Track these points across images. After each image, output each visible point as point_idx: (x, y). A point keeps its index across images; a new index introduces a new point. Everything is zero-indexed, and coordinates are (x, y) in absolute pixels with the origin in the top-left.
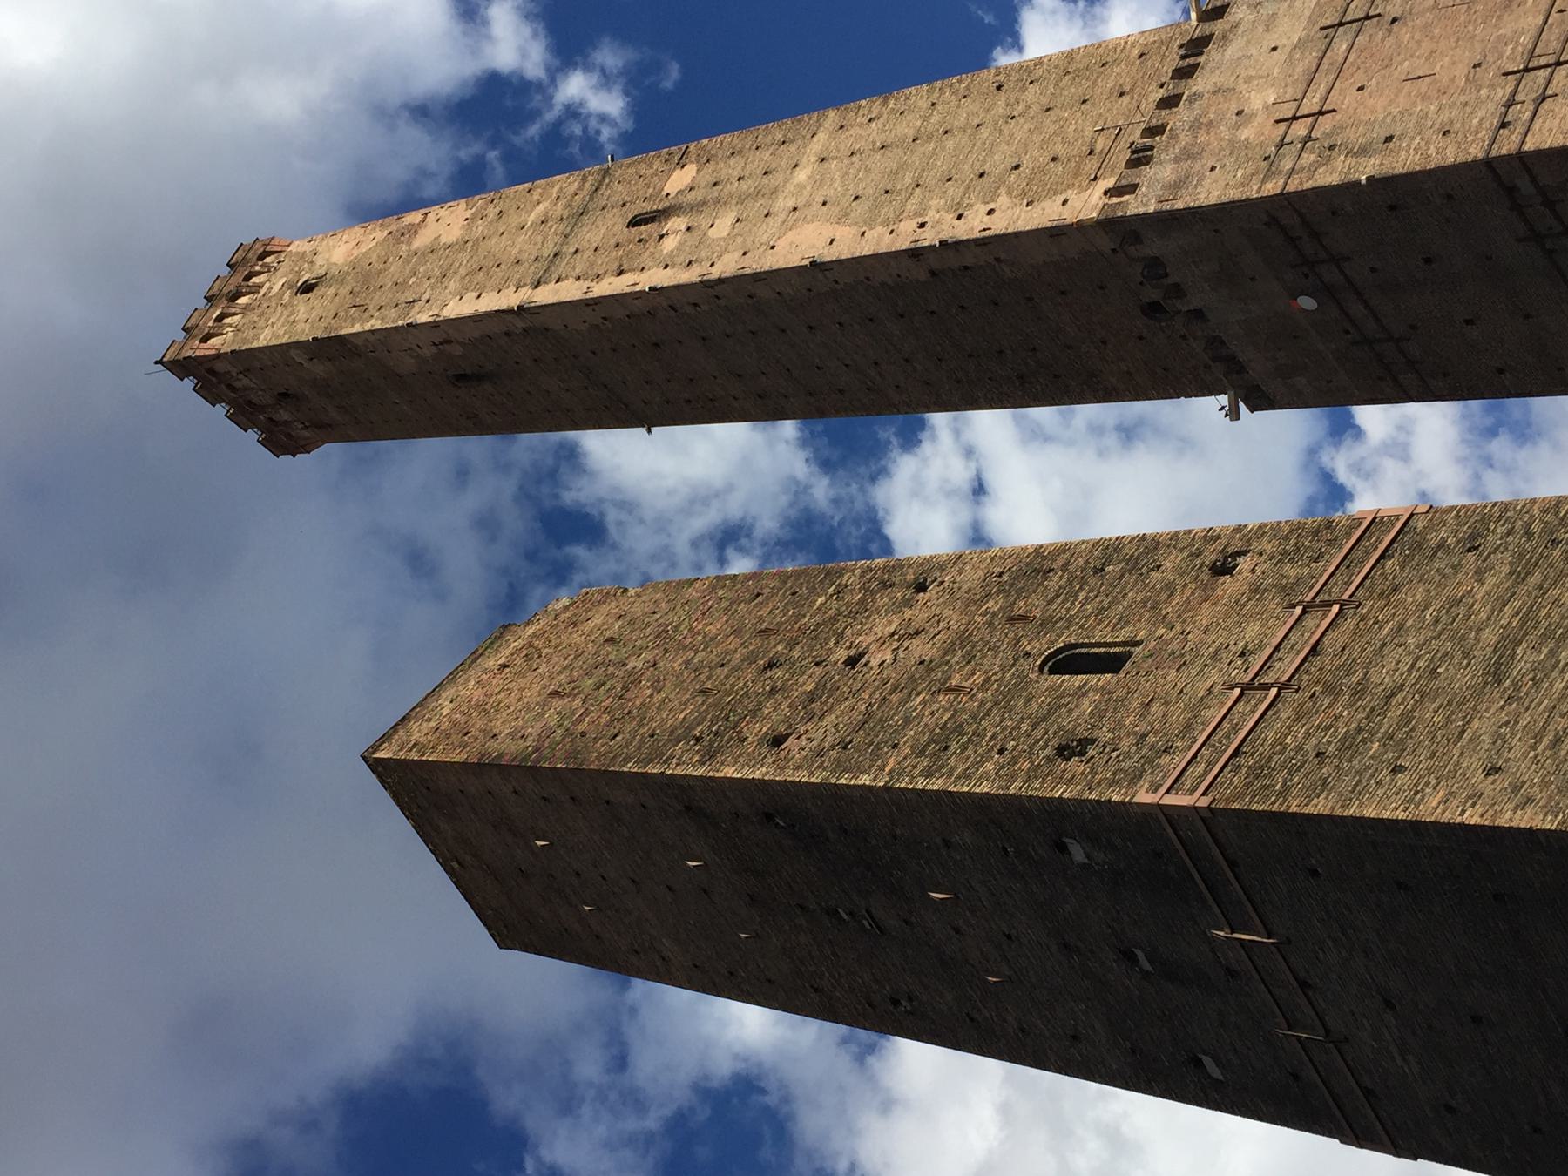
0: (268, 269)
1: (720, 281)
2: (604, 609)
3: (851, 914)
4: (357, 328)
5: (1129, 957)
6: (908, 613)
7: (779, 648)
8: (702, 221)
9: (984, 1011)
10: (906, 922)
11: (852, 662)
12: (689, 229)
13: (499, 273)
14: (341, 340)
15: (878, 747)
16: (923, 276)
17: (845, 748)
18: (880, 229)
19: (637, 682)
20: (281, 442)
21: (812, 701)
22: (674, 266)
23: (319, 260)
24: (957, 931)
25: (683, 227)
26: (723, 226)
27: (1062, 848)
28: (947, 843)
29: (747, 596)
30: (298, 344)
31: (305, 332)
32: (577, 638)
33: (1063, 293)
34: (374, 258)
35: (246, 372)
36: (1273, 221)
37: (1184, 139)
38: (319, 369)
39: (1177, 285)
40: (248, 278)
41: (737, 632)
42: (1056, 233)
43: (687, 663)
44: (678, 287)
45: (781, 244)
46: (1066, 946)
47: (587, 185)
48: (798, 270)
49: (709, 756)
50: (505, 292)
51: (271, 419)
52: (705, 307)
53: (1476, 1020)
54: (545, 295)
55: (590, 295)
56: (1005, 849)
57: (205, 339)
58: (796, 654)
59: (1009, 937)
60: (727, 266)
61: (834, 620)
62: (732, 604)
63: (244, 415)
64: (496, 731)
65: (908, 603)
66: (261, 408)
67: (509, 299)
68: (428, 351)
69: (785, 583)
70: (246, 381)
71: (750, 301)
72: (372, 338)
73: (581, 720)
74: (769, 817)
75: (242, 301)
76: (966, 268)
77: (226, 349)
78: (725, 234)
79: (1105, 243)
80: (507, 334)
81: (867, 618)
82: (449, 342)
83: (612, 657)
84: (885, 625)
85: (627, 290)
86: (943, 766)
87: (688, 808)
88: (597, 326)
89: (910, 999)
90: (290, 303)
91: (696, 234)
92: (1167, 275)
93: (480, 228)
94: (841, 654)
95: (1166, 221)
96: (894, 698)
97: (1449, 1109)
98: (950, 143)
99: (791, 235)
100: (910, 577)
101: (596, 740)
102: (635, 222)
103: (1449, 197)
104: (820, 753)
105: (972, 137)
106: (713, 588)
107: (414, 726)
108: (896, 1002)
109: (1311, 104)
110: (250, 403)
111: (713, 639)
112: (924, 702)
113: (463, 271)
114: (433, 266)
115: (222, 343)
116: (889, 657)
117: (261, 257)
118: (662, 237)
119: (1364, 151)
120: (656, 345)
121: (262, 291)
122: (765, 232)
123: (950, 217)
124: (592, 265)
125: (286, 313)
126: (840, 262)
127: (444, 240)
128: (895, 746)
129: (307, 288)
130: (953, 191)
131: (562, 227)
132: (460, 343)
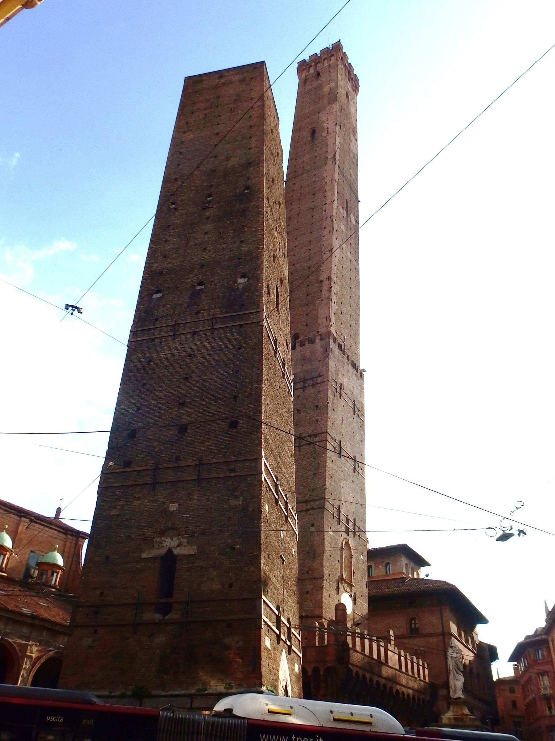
1: (332, 221)
3: (210, 201)
5: (200, 284)
8: (344, 221)
9: (172, 231)
10: (208, 218)
16: (321, 278)
23: (352, 102)
24: (206, 233)
26: (343, 227)
27: (243, 277)
28: (242, 242)
31: (340, 90)
33: (307, 314)
35: (330, 66)
36: (320, 376)
37: (341, 359)
39: (304, 345)
42: (328, 319)
48: (331, 245)
51: (311, 66)
52: (324, 213)
53: (187, 379)
56: (241, 259)
59: (205, 249)
63: (315, 59)
66: (316, 65)
67: (337, 157)
68: (326, 126)
74: (247, 188)
79: (322, 330)
80: (327, 152)
82: (328, 133)
87: (250, 163)
88: (324, 179)
89: (175, 209)
92: (309, 343)
93: (352, 156)
95: (326, 350)
97: (150, 361)
98: (348, 297)
103: (317, 421)
105: (348, 304)
108: (173, 203)
109: (343, 393)
110: (319, 62)
119: (333, 403)
120: (314, 194)
123: (335, 291)
129: (347, 96)
130: (340, 294)
132: (326, 137)
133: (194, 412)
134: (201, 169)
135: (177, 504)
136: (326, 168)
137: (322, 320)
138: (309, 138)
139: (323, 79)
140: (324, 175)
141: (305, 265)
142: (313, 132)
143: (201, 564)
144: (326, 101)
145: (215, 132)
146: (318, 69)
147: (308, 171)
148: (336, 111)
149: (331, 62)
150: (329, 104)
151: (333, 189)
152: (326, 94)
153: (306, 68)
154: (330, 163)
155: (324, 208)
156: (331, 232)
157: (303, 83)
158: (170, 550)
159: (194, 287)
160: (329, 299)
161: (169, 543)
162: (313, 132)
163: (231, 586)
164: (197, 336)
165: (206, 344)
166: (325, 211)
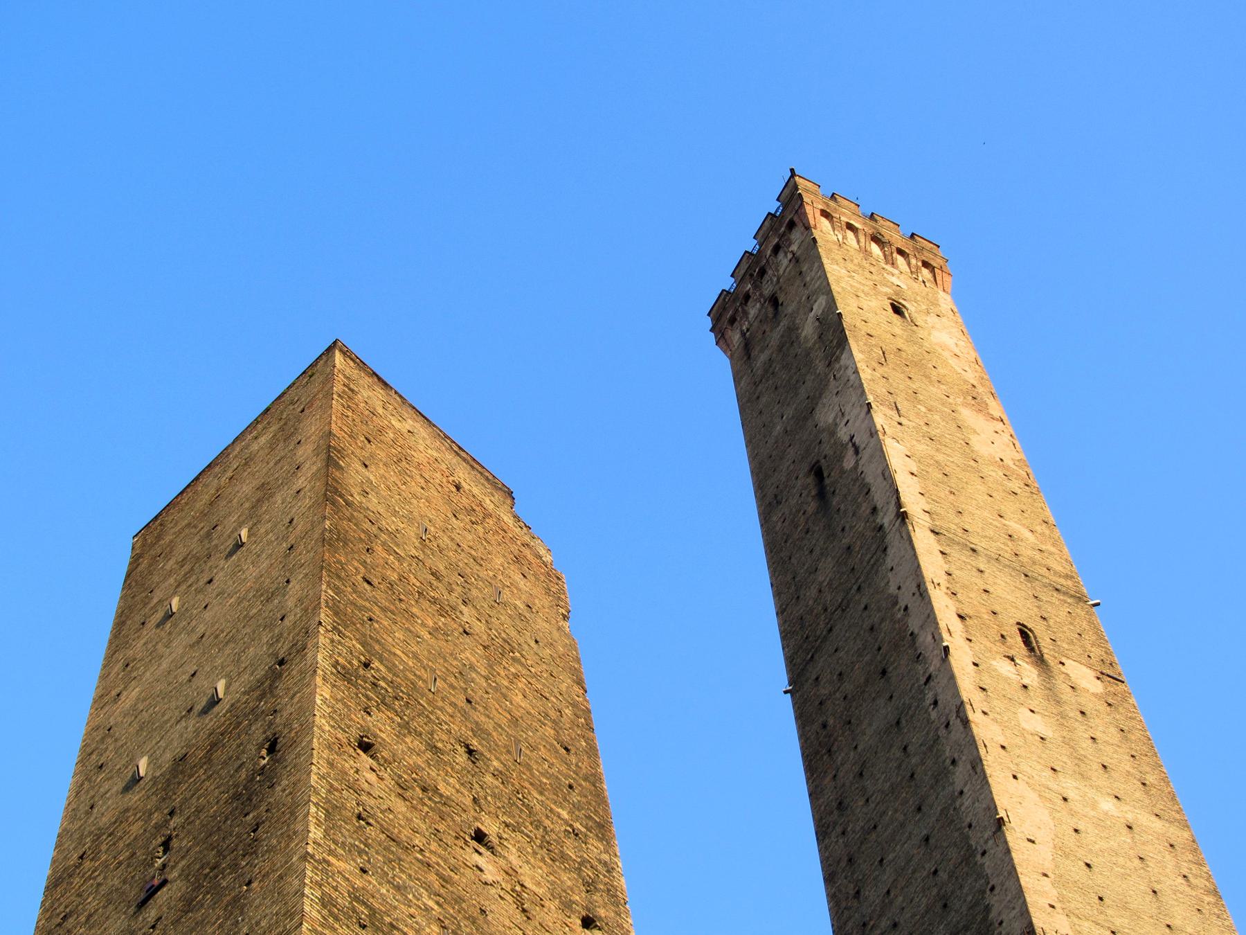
0: (914, 273)
1: (966, 722)
2: (538, 591)
4: (858, 356)
6: (552, 905)
7: (495, 763)
11: (480, 837)
12: (1025, 687)
13: (943, 493)
14: (842, 342)
15: (361, 852)
17: (359, 817)
18: (1055, 892)
19: (442, 612)
20: (725, 315)
21: (424, 790)
22: (979, 672)
23: (932, 319)
25: (1026, 681)
26: (1038, 724)
29: (566, 739)
30: (832, 302)
31: (846, 307)
32: (498, 561)
34: (941, 371)
35: (796, 260)
38: (808, 330)
40: (900, 252)
41: (514, 721)
43: (472, 667)
44: (952, 677)
47: (1062, 581)
49: (345, 675)
50: (922, 500)
51: (747, 297)
52: (934, 715)
54: (923, 541)
55: (930, 586)
57: (825, 214)
58: (489, 779)
60: (984, 729)
61: (538, 825)
62: (554, 722)
63: (752, 268)
64: (372, 468)
65: (567, 906)
69: (586, 779)
70: (785, 262)
71: (948, 762)
72: (850, 372)
73: (389, 551)
75: (875, 249)
77: (816, 234)
78: (1024, 725)
80: (874, 510)
81: (543, 860)
82: (857, 452)
83: (475, 592)
84: (534, 876)
85: (942, 625)
86: (336, 919)
87: (281, 663)
88: (896, 603)
90: (878, 293)
91: (1021, 694)
94: (491, 828)
96: (432, 877)
99: (1032, 796)
100: (602, 912)
101: (364, 563)
102: (1025, 633)
104: (354, 788)
106: (574, 705)
107: (380, 392)
110: (763, 272)
111: (505, 697)
112: (428, 909)
113: (940, 457)
114: (940, 427)
115: (823, 230)
116: (488, 877)
117: (926, 264)
118: (1012, 660)
120: (884, 672)
121: (888, 267)
122: (1033, 768)
124: (964, 587)
125: (866, 289)
126: (1008, 851)
127: (975, 441)
128: (364, 871)
131: (1007, 555)
136: (889, 562)
138: (812, 507)
139: (790, 310)
140: (892, 589)
144: (820, 367)
145: (195, 638)
146: (767, 290)
147: (843, 608)
148: (856, 372)
149: (794, 248)
150: (829, 365)
151: (930, 617)
152: (810, 344)
153: (737, 310)
154: (892, 538)
156: (977, 765)
166: (935, 703)
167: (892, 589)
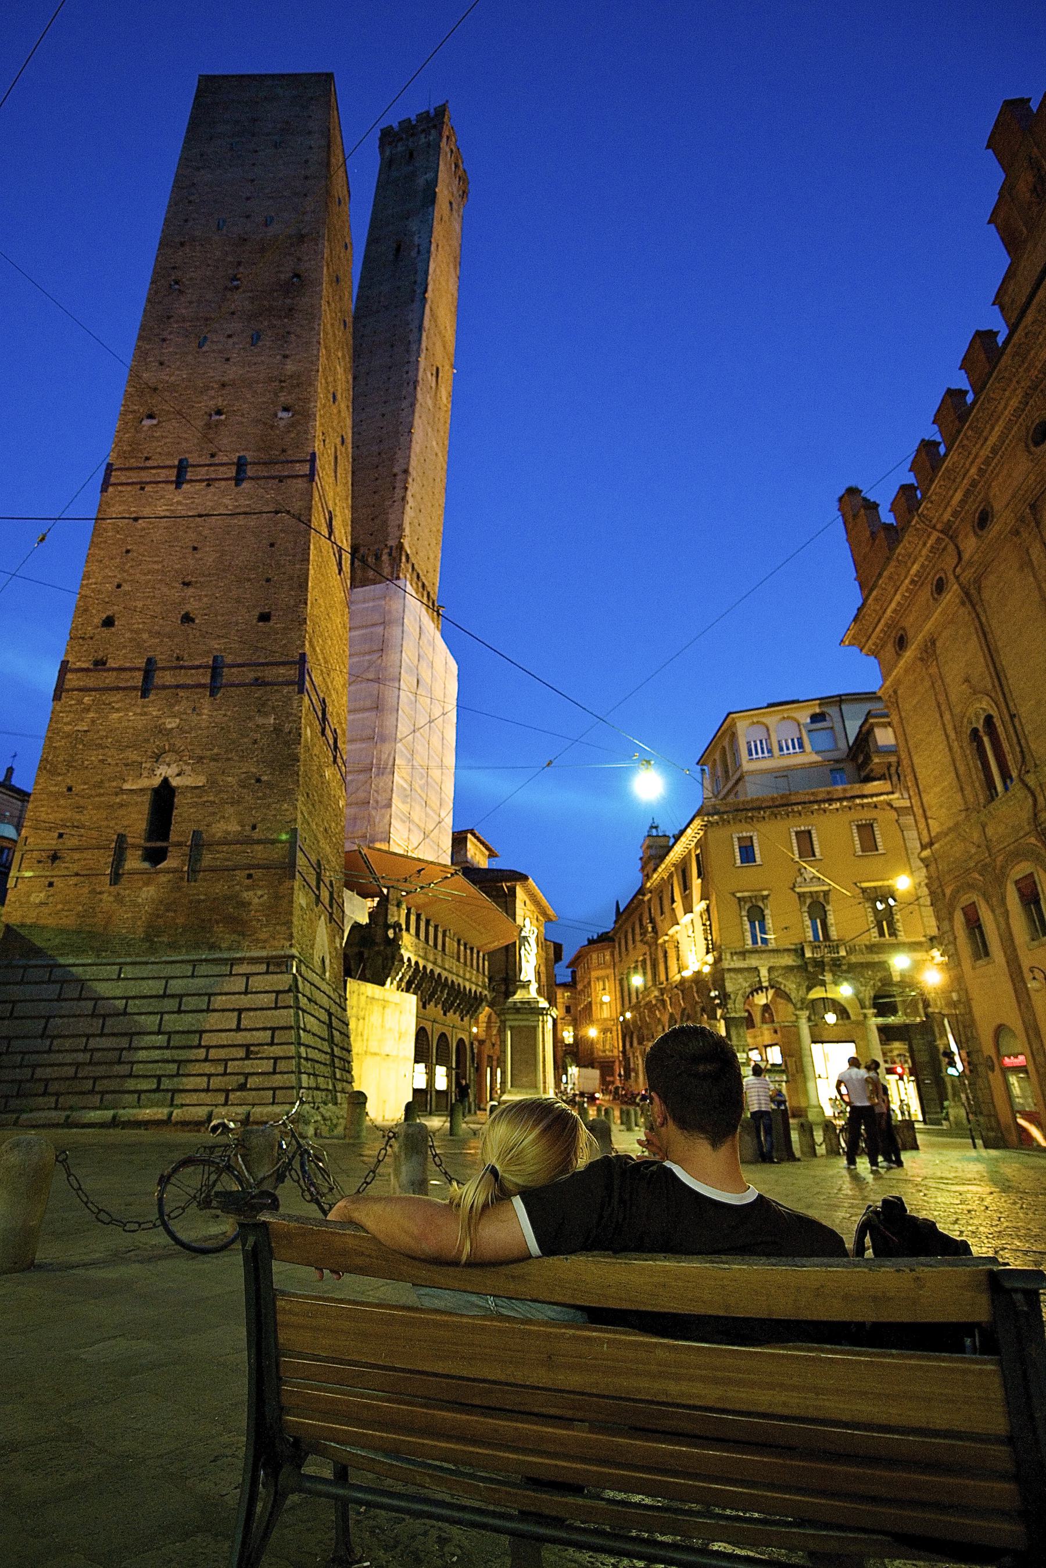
1: (415, 388)
5: (219, 412)
10: (233, 313)
16: (395, 470)
24: (230, 336)
26: (430, 402)
38: (421, 181)
42: (400, 527)
45: (420, 421)
46: (223, 385)
53: (195, 549)
57: (448, 137)
59: (228, 360)
63: (408, 128)
70: (423, 140)
76: (394, 488)
79: (392, 543)
80: (415, 282)
82: (419, 252)
98: (430, 505)
102: (437, 369)
130: (419, 497)
132: (415, 258)
133: (206, 596)
134: (224, 232)
135: (178, 720)
137: (393, 531)
138: (391, 257)
140: (409, 318)
141: (375, 449)
142: (398, 249)
143: (212, 798)
155: (406, 368)
156: (413, 405)
157: (388, 164)
158: (166, 781)
159: (211, 415)
160: (404, 498)
161: (164, 771)
162: (398, 249)
163: (254, 827)
164: (212, 489)
165: (228, 502)
166: (407, 373)
167: (409, 318)
